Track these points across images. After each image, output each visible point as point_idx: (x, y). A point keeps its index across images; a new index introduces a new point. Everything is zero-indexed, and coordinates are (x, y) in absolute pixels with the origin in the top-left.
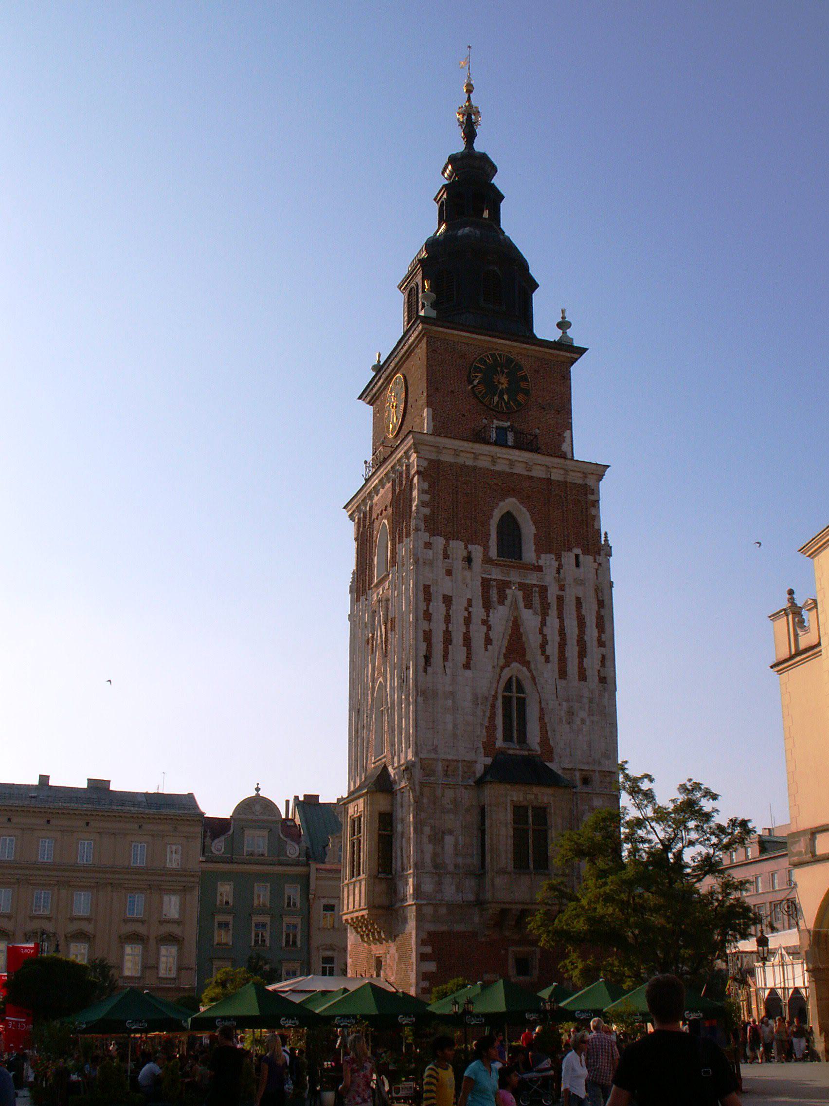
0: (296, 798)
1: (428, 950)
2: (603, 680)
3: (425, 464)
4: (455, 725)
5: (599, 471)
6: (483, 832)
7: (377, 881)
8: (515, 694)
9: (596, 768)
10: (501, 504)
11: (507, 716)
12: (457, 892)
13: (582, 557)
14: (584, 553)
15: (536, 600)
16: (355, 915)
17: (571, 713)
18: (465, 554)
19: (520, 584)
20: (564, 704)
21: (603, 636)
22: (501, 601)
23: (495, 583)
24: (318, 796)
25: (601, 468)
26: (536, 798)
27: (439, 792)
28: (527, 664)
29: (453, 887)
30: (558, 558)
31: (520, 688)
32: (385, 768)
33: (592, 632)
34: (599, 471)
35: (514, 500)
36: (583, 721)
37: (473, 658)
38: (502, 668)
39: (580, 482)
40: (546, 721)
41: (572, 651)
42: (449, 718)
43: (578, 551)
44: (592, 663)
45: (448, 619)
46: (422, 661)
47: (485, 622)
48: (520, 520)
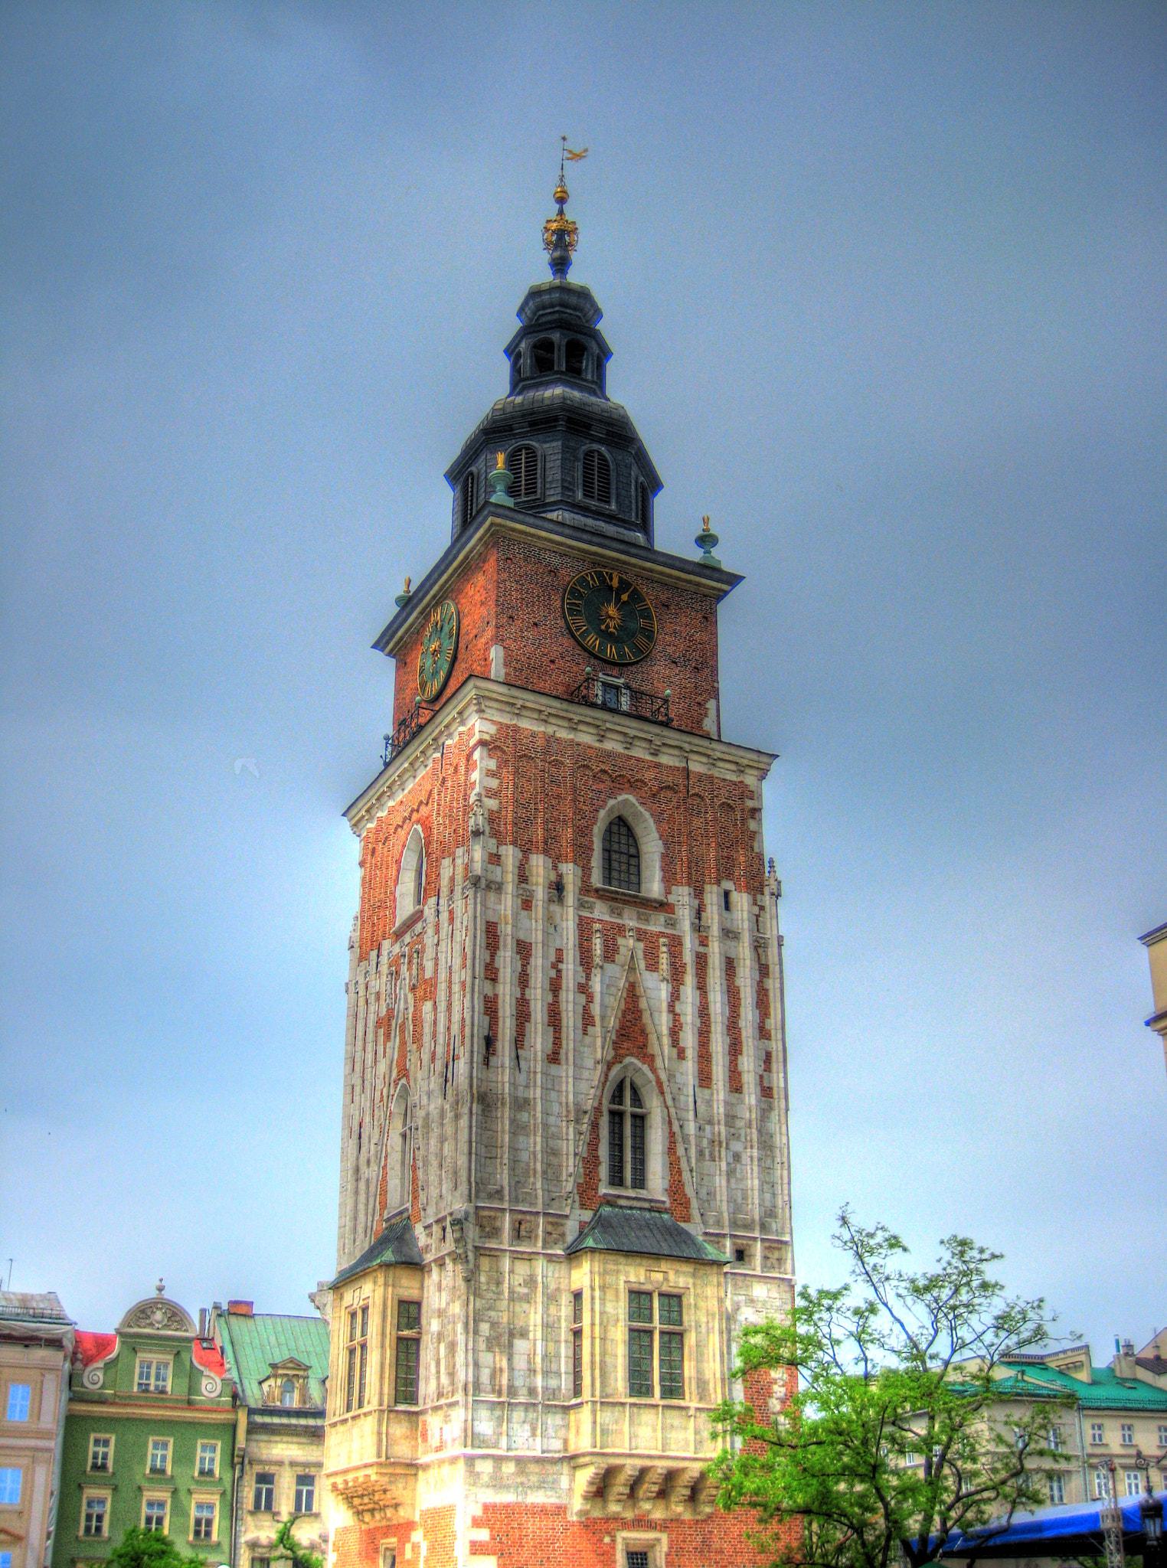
0: (216, 1307)
1: (483, 1535)
2: (766, 1092)
3: (492, 729)
6: (577, 1333)
7: (392, 1416)
8: (628, 1107)
9: (756, 1234)
10: (611, 802)
11: (617, 1145)
12: (534, 1435)
13: (735, 897)
14: (738, 889)
15: (664, 959)
16: (350, 1477)
18: (553, 877)
19: (639, 930)
20: (708, 1127)
21: (767, 1021)
23: (597, 926)
24: (250, 1304)
25: (765, 759)
26: (666, 1279)
27: (506, 1263)
28: (649, 1059)
29: (527, 1427)
30: (699, 893)
31: (637, 1100)
32: (407, 1228)
35: (631, 798)
38: (609, 1066)
39: (733, 778)
40: (680, 1151)
43: (728, 885)
44: (748, 1064)
45: (523, 981)
46: (479, 1046)
47: (583, 989)
48: (639, 830)
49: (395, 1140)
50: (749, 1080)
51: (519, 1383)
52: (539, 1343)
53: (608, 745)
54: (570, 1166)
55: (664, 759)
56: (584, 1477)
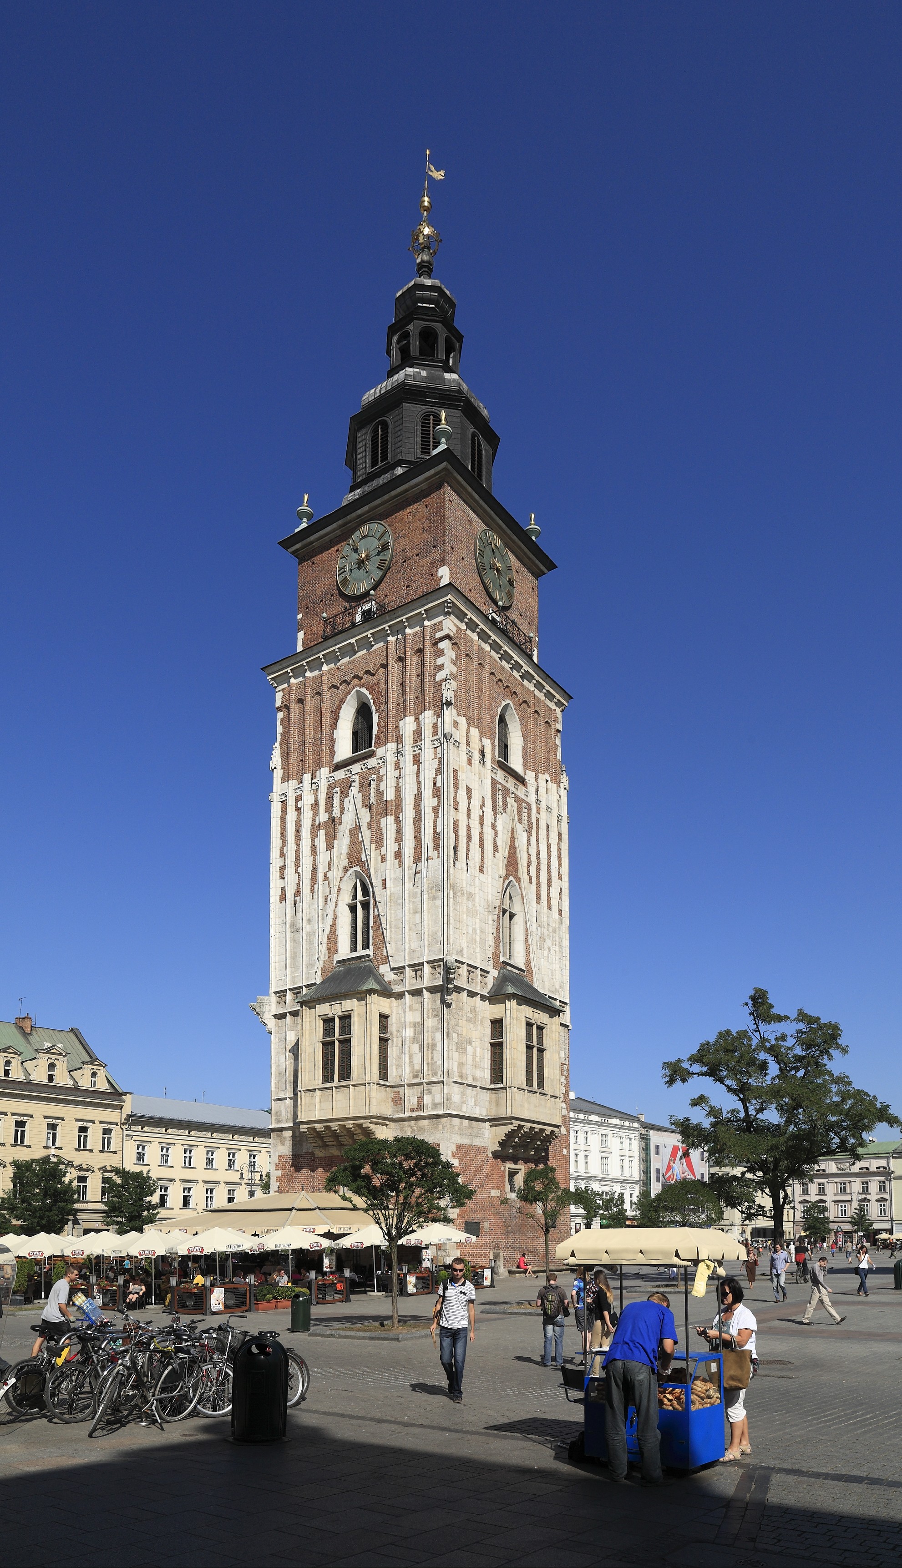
4: (474, 929)
8: (507, 908)
12: (475, 1105)
17: (543, 939)
22: (505, 810)
28: (518, 880)
36: (549, 949)
37: (485, 860)
40: (530, 942)
47: (494, 826)
50: (554, 903)
51: (468, 1073)
52: (478, 1049)
56: (502, 1132)
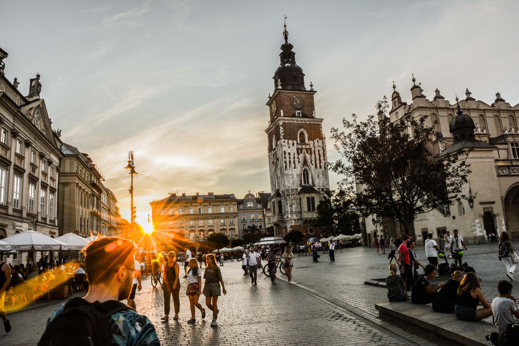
5: (321, 120)
15: (309, 152)
17: (318, 176)
28: (308, 166)
30: (313, 141)
31: (307, 171)
33: (322, 157)
34: (321, 120)
41: (318, 162)
42: (292, 180)
44: (323, 164)
45: (290, 158)
47: (298, 158)
49: (276, 179)
53: (299, 122)
54: (299, 182)
55: (307, 122)
